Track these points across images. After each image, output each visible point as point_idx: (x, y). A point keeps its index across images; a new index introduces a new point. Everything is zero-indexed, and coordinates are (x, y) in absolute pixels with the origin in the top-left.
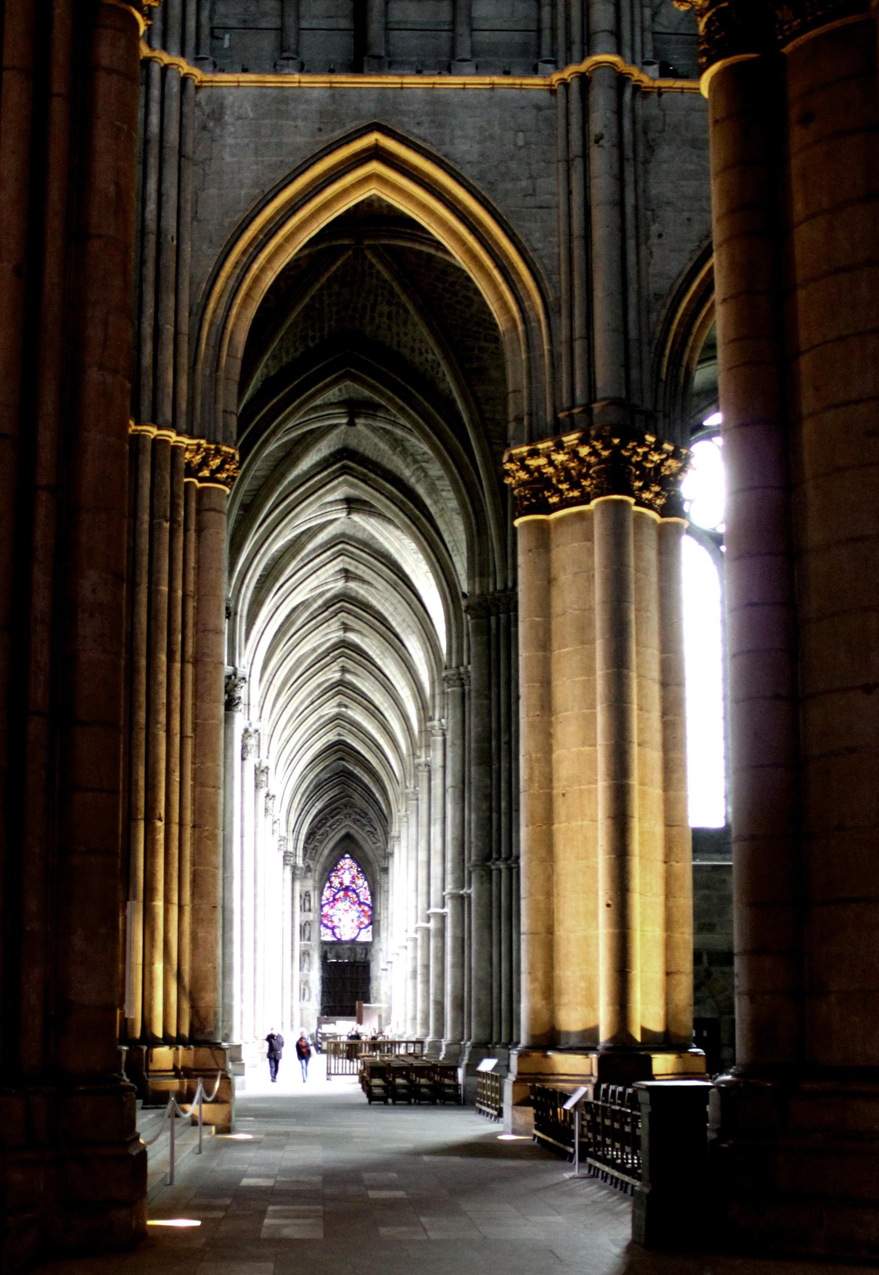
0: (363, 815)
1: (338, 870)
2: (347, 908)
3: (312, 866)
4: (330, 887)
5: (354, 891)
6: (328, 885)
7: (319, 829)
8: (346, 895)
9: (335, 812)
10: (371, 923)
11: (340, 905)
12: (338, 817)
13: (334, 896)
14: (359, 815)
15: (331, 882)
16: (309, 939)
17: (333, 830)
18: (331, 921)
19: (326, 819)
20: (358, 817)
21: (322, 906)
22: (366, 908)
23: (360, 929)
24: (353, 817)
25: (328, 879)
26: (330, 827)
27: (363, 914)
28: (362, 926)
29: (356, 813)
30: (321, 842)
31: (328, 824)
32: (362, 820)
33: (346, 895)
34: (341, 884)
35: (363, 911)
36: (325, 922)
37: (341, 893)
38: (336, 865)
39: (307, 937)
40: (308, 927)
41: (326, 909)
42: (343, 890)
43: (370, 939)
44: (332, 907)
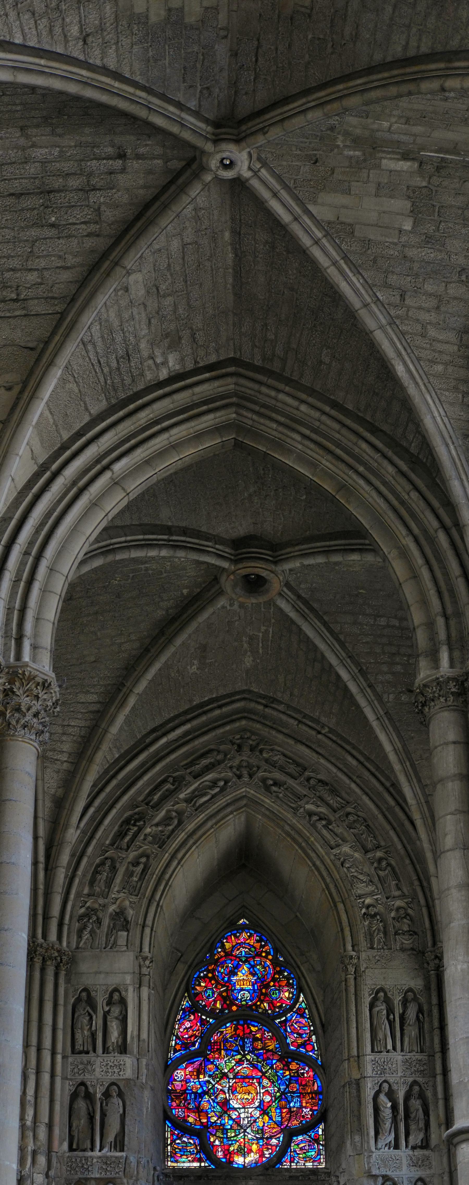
0: (292, 769)
1: (218, 963)
2: (245, 1069)
3: (130, 913)
4: (194, 1009)
5: (266, 1020)
6: (185, 1004)
7: (157, 806)
8: (241, 1037)
9: (205, 762)
10: (322, 1117)
11: (226, 1064)
12: (210, 776)
13: (205, 1037)
14: (282, 769)
15: (195, 997)
16: (120, 1144)
17: (199, 809)
18: (198, 1110)
19: (179, 783)
20: (278, 775)
21: (169, 1068)
22: (307, 1072)
23: (290, 1134)
24: (261, 774)
25: (188, 988)
26: (188, 801)
27: (295, 1086)
28: (295, 1123)
29: (267, 761)
30: (161, 842)
31: (182, 796)
32: (290, 782)
33: (241, 1037)
34: (228, 999)
35: (297, 1078)
36: (178, 1112)
37: (228, 1030)
38: (212, 949)
39: (111, 1138)
40: (116, 1101)
41: (179, 1074)
42: (233, 1018)
43: (323, 1166)
44: (199, 1071)
